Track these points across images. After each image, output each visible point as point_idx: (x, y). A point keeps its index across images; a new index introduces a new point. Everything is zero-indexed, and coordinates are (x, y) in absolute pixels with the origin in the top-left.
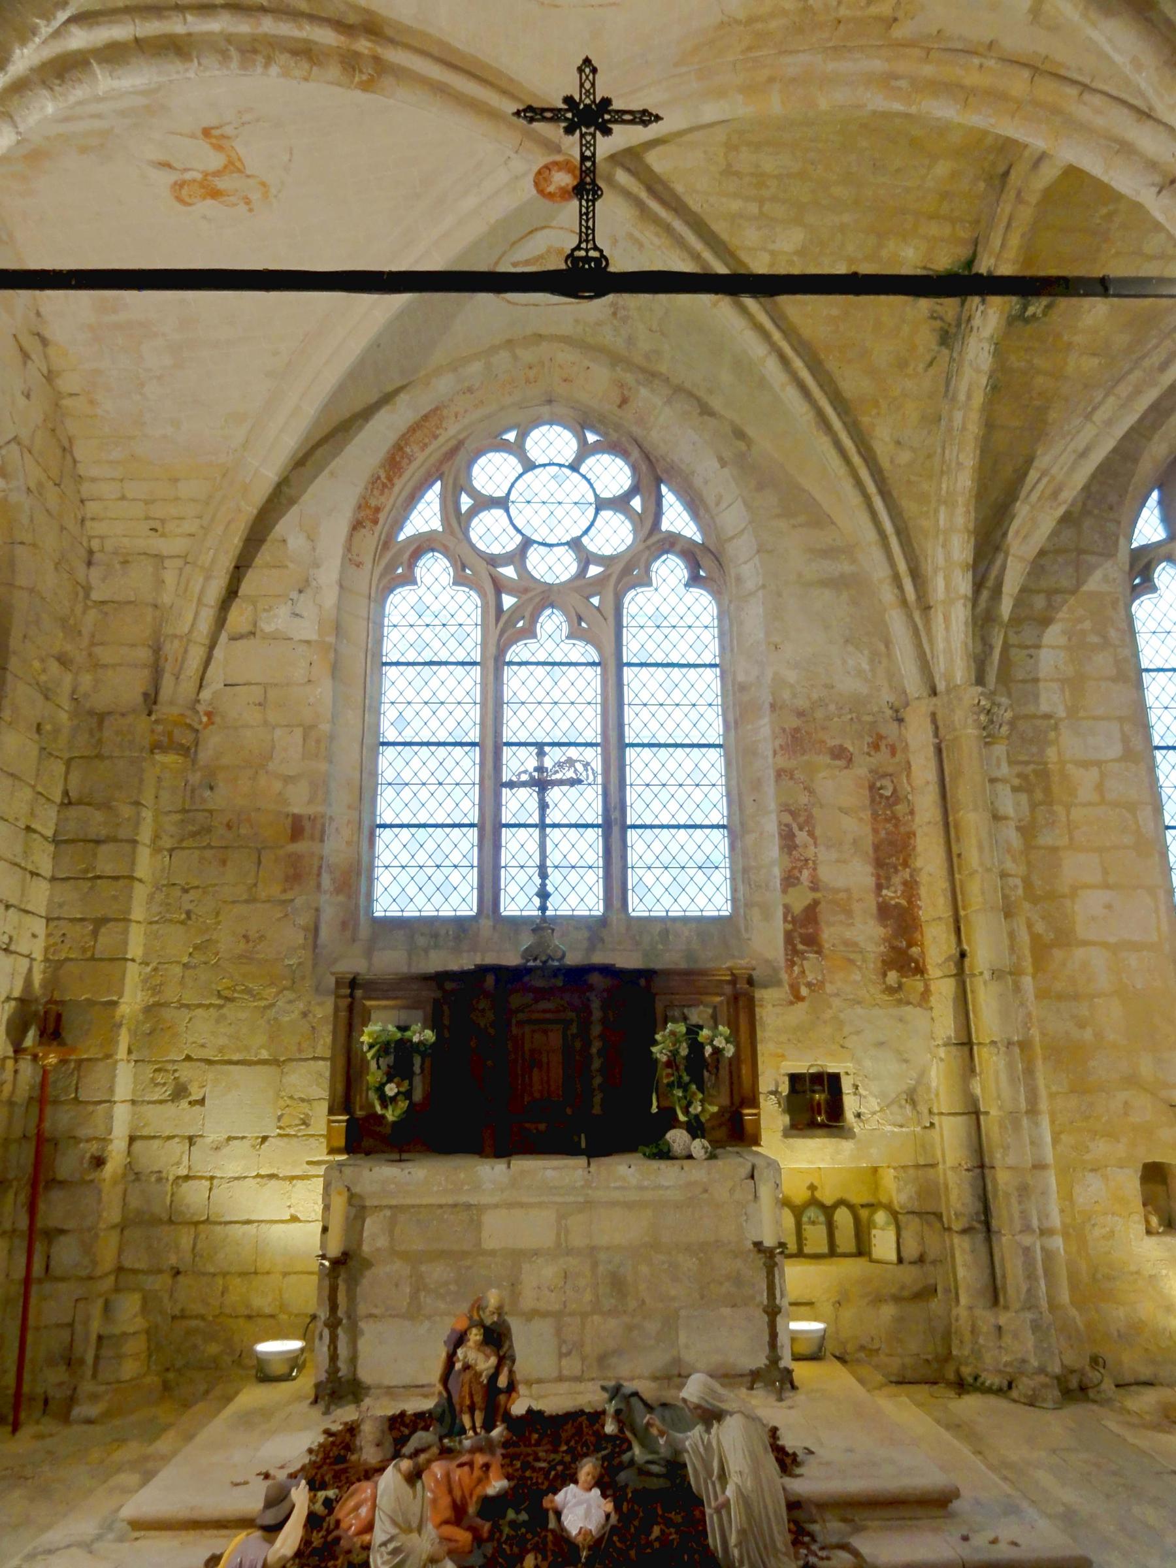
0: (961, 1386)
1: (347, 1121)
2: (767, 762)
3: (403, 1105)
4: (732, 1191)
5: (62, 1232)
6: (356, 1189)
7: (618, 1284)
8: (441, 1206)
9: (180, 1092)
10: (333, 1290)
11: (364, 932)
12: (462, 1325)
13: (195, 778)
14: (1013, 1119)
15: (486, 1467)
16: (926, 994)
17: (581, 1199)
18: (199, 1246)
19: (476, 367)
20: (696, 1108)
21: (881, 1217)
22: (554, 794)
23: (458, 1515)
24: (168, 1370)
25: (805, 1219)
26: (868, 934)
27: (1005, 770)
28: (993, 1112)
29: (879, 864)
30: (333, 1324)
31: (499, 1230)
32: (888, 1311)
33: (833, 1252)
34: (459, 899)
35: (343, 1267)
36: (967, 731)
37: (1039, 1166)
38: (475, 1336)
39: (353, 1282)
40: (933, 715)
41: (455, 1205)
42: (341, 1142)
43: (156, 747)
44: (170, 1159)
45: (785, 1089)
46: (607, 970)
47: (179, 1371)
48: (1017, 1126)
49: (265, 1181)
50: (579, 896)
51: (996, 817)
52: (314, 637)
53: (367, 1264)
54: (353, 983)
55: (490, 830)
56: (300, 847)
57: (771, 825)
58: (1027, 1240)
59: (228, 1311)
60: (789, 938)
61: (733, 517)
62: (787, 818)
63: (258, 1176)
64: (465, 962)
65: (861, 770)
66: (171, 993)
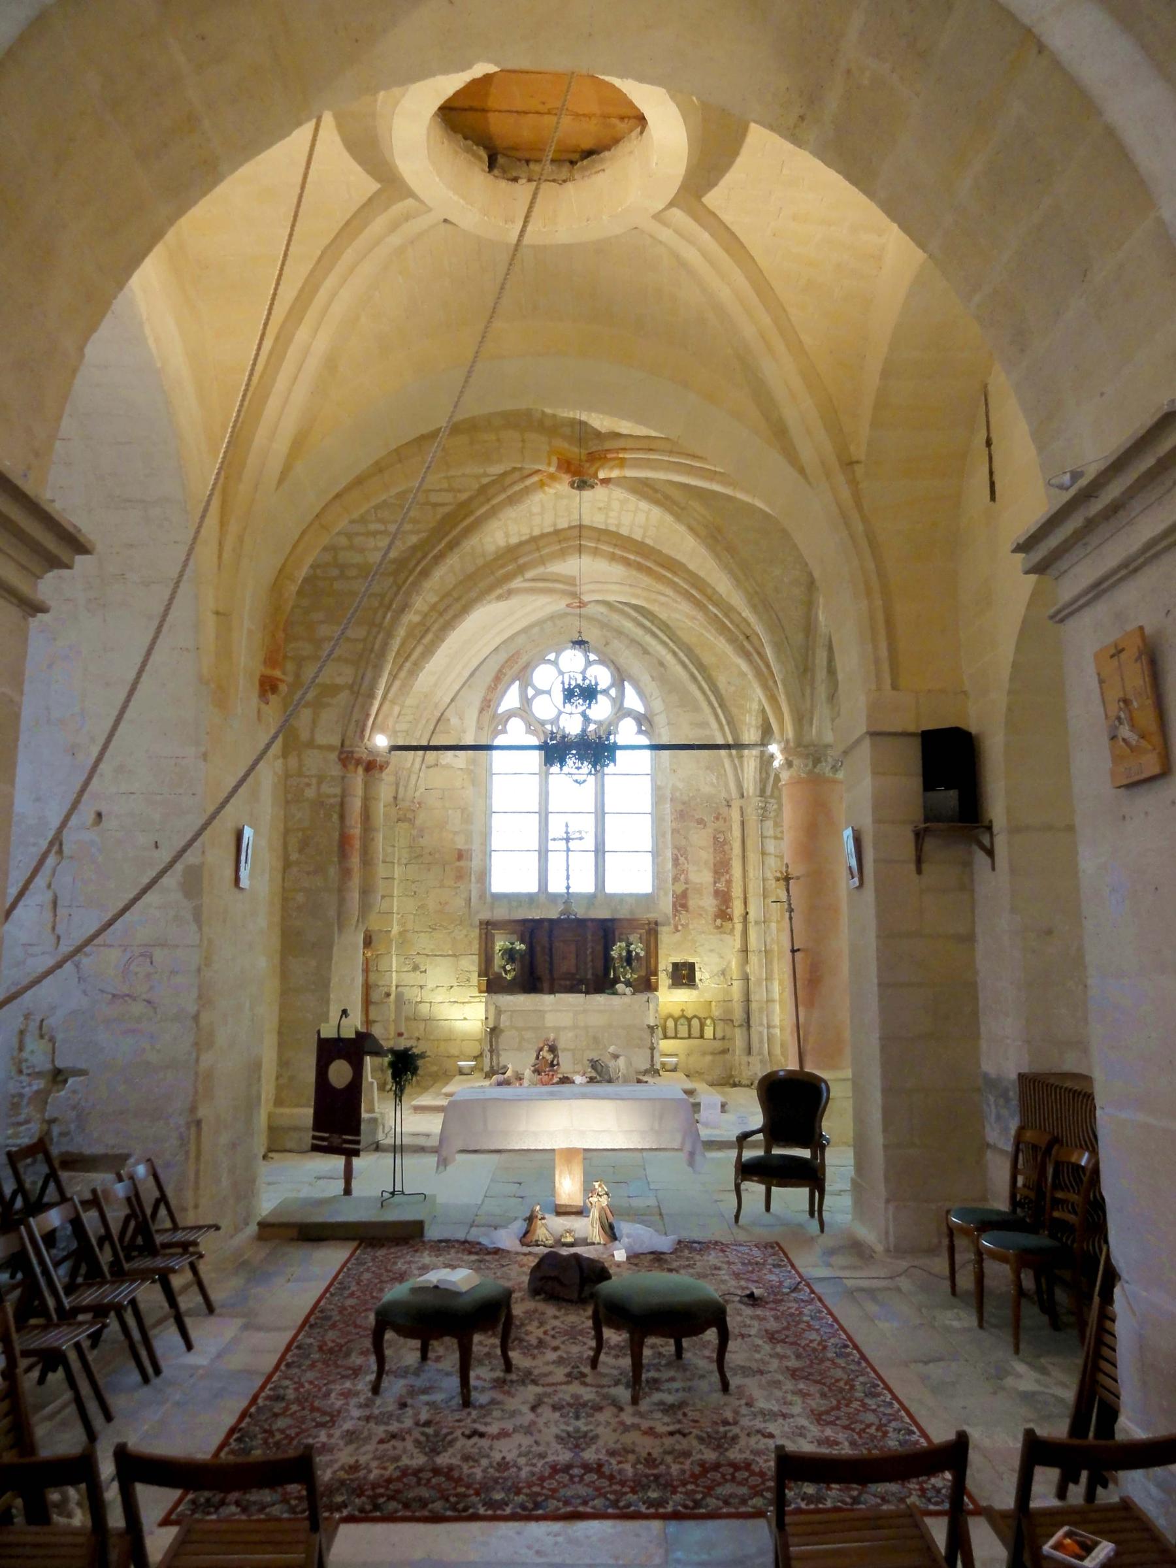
0: (735, 1085)
2: (668, 825)
3: (513, 973)
5: (375, 1022)
7: (596, 1039)
9: (416, 968)
11: (489, 900)
13: (415, 832)
14: (759, 981)
16: (733, 929)
19: (536, 630)
20: (628, 976)
21: (708, 1022)
22: (572, 845)
26: (709, 903)
27: (771, 833)
28: (752, 978)
29: (716, 872)
31: (551, 1020)
32: (709, 1058)
33: (690, 1037)
34: (530, 886)
35: (494, 1032)
36: (752, 818)
37: (769, 1001)
38: (546, 1048)
39: (497, 1037)
40: (741, 808)
42: (484, 988)
43: (399, 820)
44: (412, 994)
45: (670, 969)
46: (592, 920)
48: (760, 985)
50: (584, 884)
51: (763, 853)
52: (463, 766)
53: (502, 1031)
54: (488, 923)
55: (543, 854)
56: (462, 863)
57: (669, 854)
58: (760, 1029)
60: (674, 905)
61: (658, 705)
62: (676, 852)
64: (536, 915)
65: (709, 831)
66: (409, 926)
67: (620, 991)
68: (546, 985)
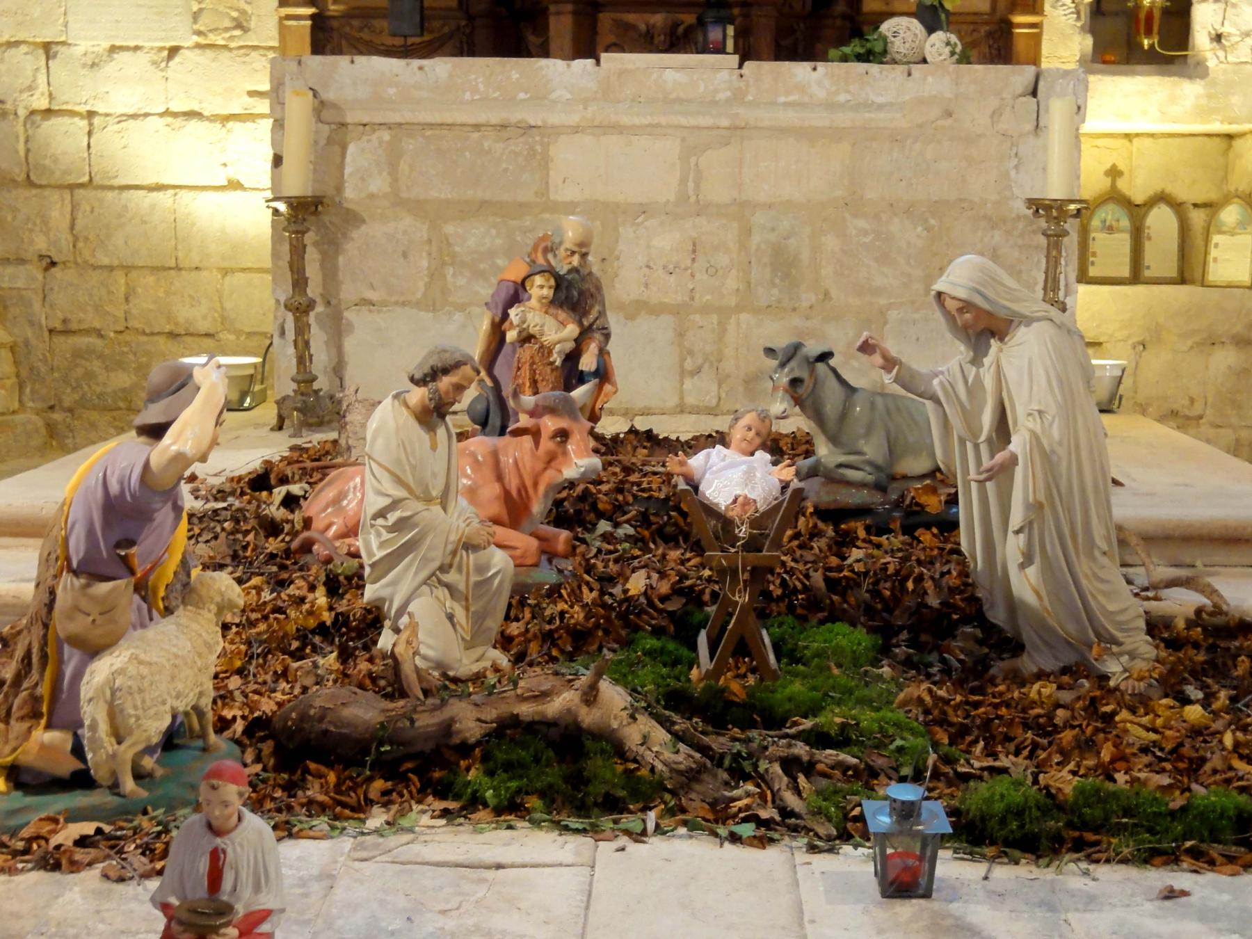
1: (313, 17)
4: (996, 114)
6: (329, 95)
7: (784, 265)
8: (477, 127)
10: (298, 252)
12: (516, 272)
15: (563, 435)
17: (725, 122)
18: (80, 223)
23: (514, 510)
24: (52, 408)
25: (1095, 223)
30: (300, 309)
32: (1225, 359)
33: (1136, 278)
35: (308, 217)
38: (540, 288)
39: (332, 247)
41: (504, 126)
47: (70, 410)
49: (179, 122)
53: (353, 219)
59: (135, 324)
63: (167, 113)
67: (899, 46)
68: (561, 25)
